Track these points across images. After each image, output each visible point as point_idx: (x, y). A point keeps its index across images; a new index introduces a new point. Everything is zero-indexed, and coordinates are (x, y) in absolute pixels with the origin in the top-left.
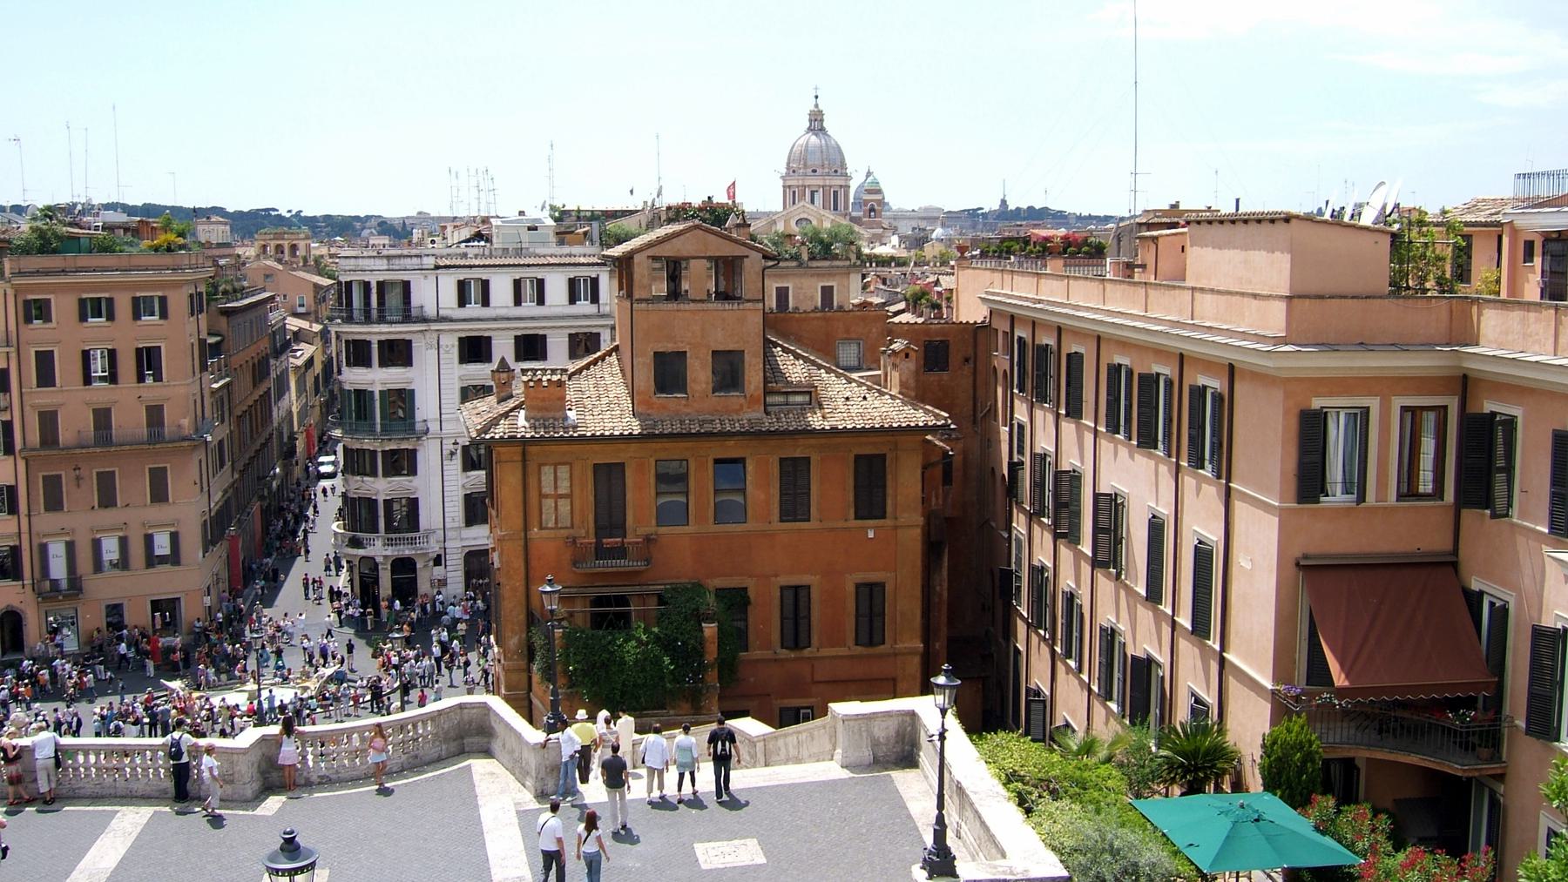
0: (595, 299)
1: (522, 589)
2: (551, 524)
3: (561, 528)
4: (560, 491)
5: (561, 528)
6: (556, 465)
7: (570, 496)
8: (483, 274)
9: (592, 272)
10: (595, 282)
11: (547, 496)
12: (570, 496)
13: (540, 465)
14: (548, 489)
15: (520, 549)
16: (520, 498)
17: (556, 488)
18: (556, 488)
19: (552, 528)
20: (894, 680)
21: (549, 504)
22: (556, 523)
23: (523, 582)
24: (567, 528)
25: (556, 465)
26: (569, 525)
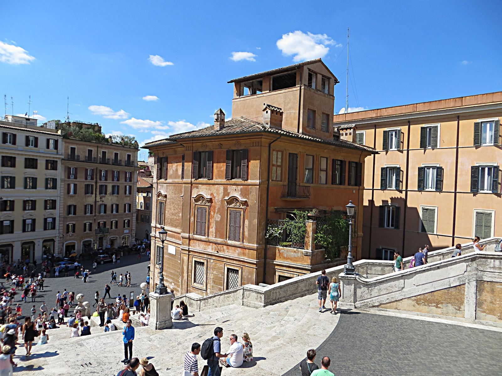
0: (56, 147)
1: (265, 209)
2: (274, 179)
3: (278, 181)
4: (279, 164)
5: (278, 181)
6: (278, 151)
7: (281, 166)
8: (14, 132)
9: (56, 138)
10: (56, 142)
11: (273, 165)
12: (281, 166)
13: (273, 150)
14: (274, 163)
15: (266, 189)
16: (267, 165)
17: (277, 162)
18: (277, 162)
19: (275, 181)
20: (357, 247)
21: (274, 168)
22: (276, 178)
23: (266, 206)
24: (279, 181)
25: (278, 151)
26: (280, 180)
